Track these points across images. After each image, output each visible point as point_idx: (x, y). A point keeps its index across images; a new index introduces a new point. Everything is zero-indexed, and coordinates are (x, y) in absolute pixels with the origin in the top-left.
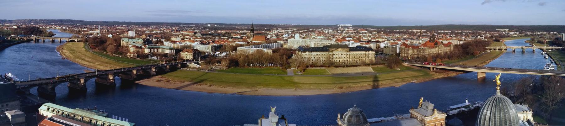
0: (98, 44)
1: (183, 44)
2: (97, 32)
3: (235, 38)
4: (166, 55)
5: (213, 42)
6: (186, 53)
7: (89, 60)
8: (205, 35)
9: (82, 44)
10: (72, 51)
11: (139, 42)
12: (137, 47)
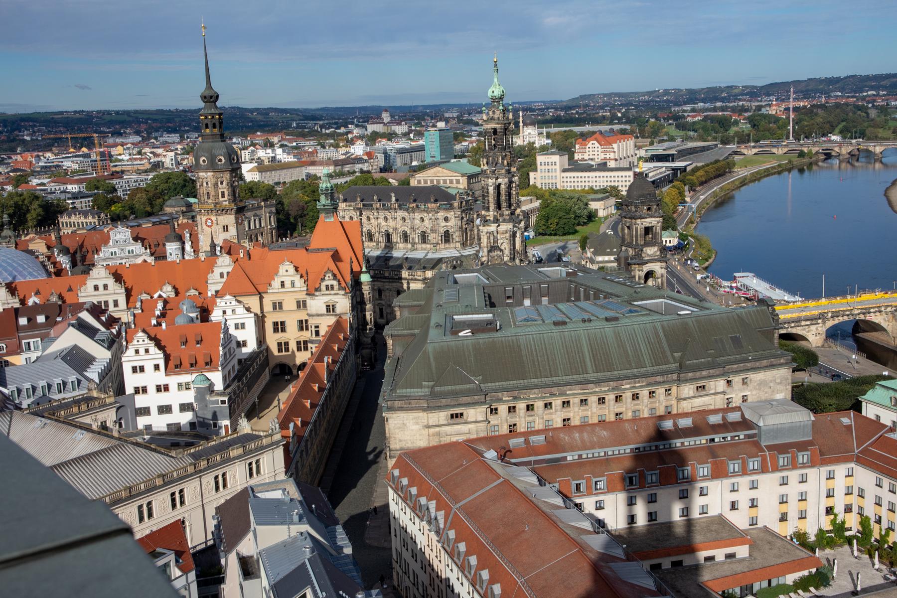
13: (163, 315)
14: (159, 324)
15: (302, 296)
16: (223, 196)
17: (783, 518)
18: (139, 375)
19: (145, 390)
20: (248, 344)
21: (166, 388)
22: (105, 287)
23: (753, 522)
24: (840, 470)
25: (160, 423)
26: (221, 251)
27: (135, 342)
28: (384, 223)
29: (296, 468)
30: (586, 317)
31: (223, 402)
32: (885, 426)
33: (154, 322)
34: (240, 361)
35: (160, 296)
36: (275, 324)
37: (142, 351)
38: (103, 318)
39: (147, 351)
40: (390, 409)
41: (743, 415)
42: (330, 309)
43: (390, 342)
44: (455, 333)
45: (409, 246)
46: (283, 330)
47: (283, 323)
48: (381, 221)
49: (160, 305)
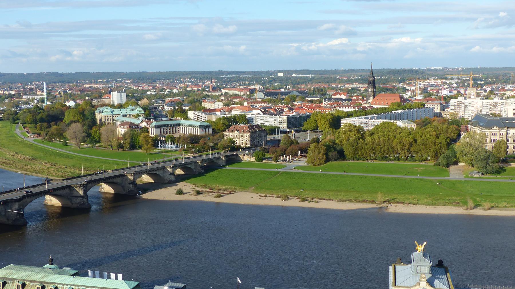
1: (228, 115)
3: (336, 99)
4: (194, 140)
5: (291, 109)
6: (236, 133)
8: (272, 96)
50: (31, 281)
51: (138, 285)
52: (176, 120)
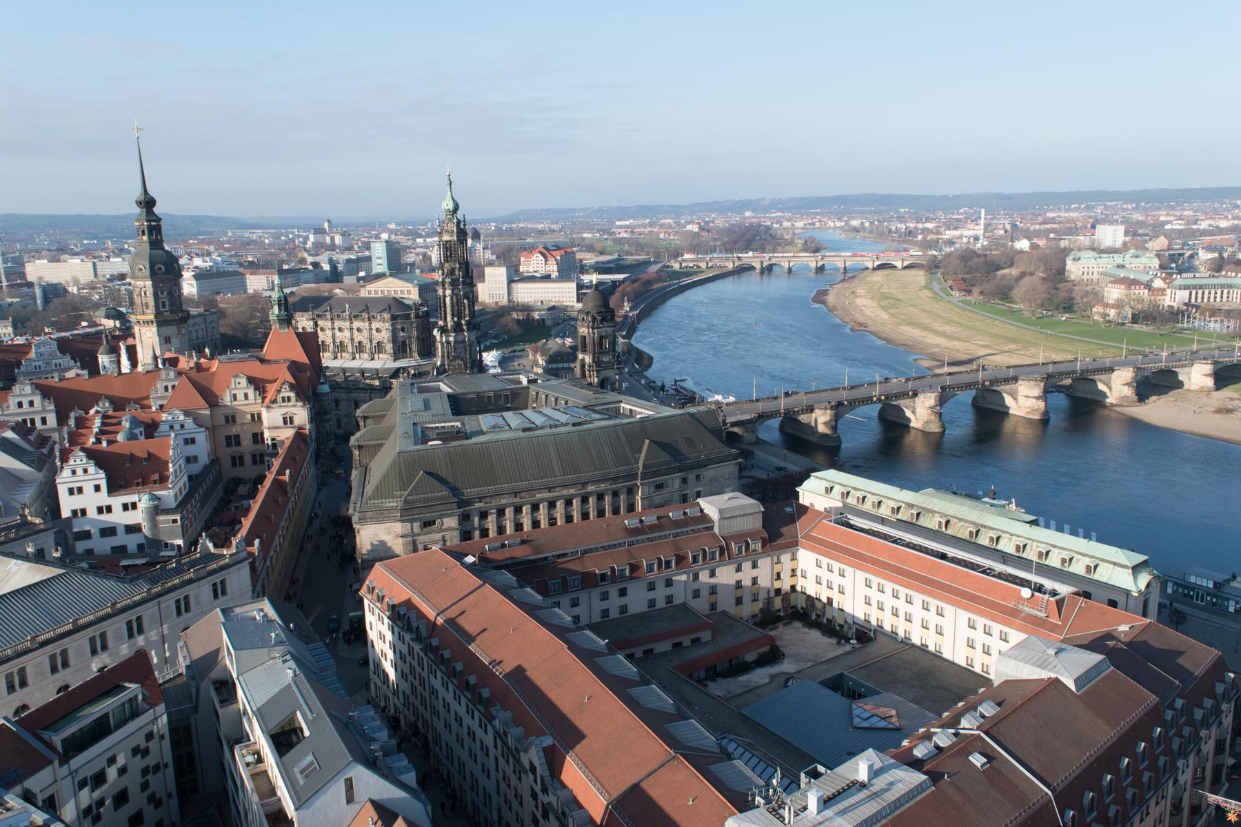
0: (978, 275)
2: (973, 235)
7: (950, 329)
9: (920, 276)
10: (885, 300)
11: (1144, 263)
12: (1131, 283)
13: (102, 432)
14: (99, 441)
15: (255, 409)
16: (164, 305)
17: (739, 601)
18: (76, 497)
19: (84, 512)
20: (200, 458)
21: (109, 509)
22: (31, 404)
23: (713, 606)
24: (786, 558)
25: (102, 546)
26: (164, 364)
27: (71, 462)
28: (338, 334)
29: (263, 585)
30: (552, 423)
31: (175, 521)
32: (821, 513)
33: (92, 440)
34: (190, 478)
35: (97, 412)
36: (228, 438)
37: (80, 471)
38: (31, 438)
39: (85, 471)
40: (362, 520)
41: (702, 510)
42: (288, 421)
43: (356, 452)
44: (425, 442)
45: (366, 356)
46: (238, 443)
47: (237, 437)
48: (337, 331)
49: (98, 422)
50: (960, 520)
51: (1145, 561)
52: (1225, 276)
